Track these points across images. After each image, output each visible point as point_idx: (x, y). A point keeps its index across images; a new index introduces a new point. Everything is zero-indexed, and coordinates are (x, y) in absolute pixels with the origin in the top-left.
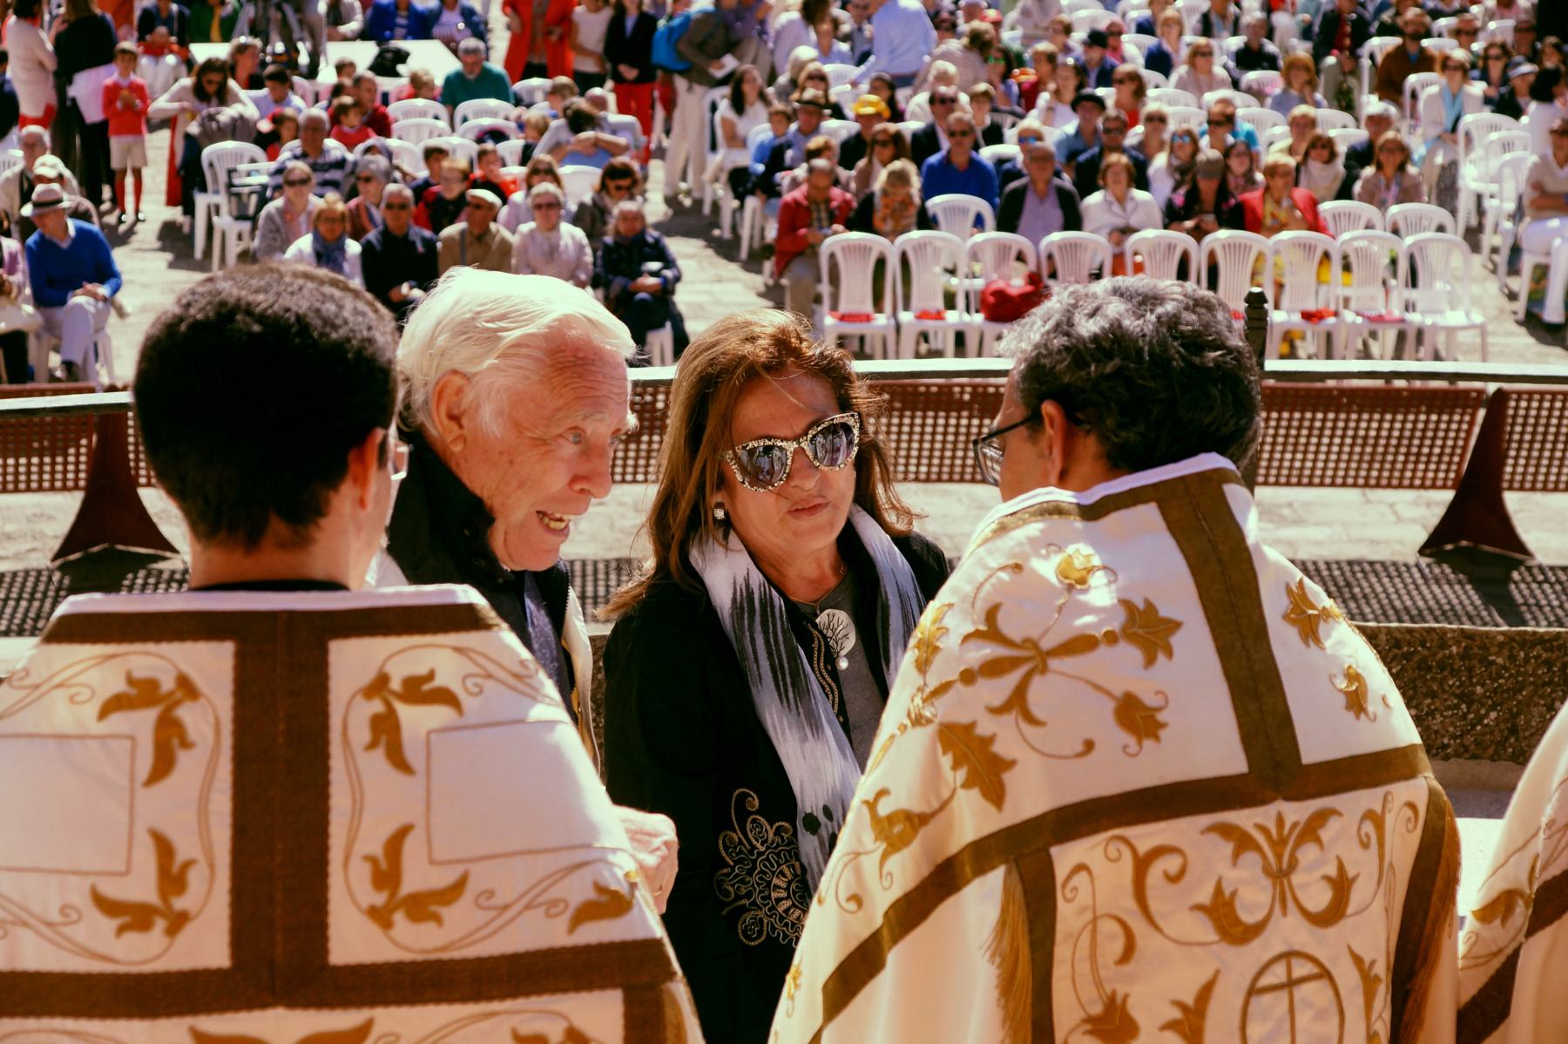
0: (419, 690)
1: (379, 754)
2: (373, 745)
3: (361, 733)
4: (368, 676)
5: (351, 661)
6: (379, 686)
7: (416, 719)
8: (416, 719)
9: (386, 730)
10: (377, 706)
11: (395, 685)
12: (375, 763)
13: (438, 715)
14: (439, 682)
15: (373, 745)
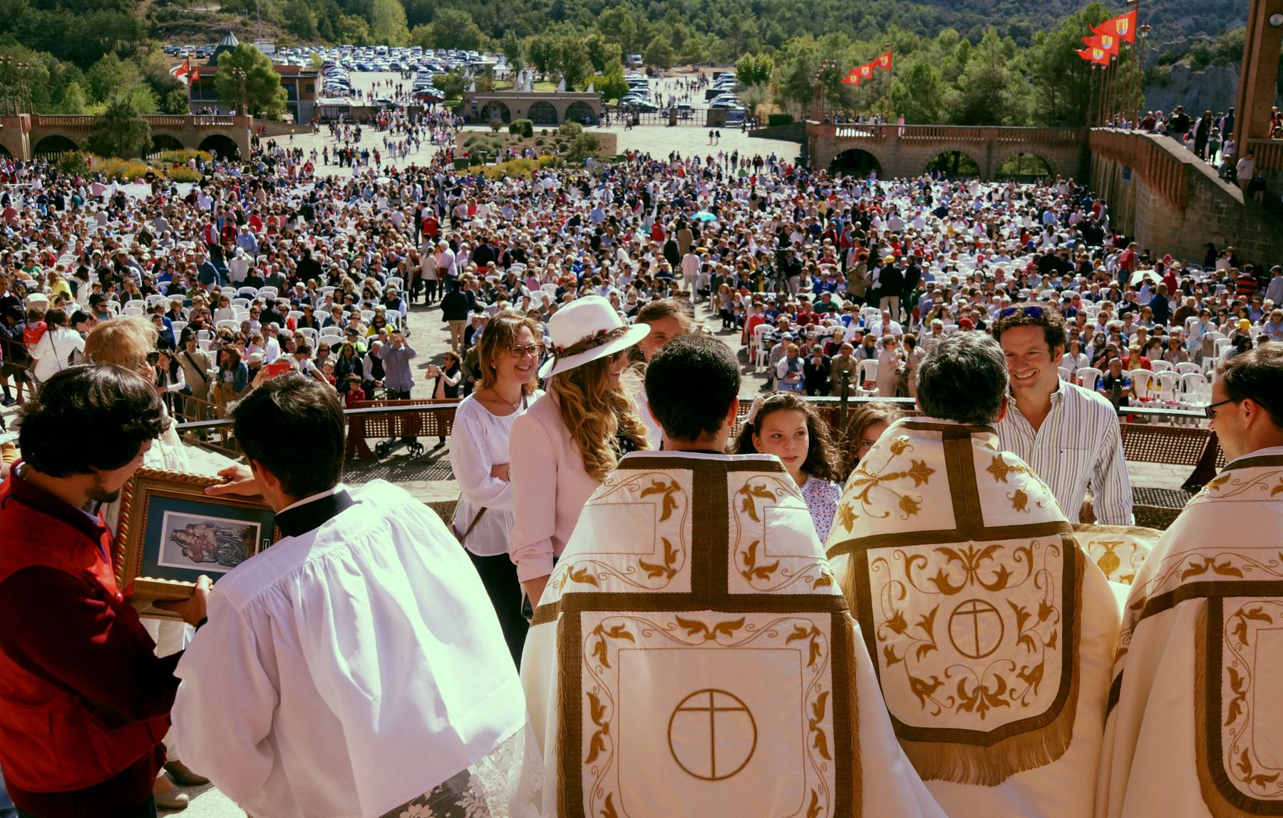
0: (760, 492)
1: (747, 514)
2: (744, 510)
3: (739, 504)
4: (741, 486)
5: (735, 480)
6: (745, 489)
7: (759, 502)
8: (759, 502)
9: (749, 506)
10: (745, 496)
11: (752, 489)
12: (745, 518)
13: (767, 501)
14: (768, 489)
15: (744, 510)
